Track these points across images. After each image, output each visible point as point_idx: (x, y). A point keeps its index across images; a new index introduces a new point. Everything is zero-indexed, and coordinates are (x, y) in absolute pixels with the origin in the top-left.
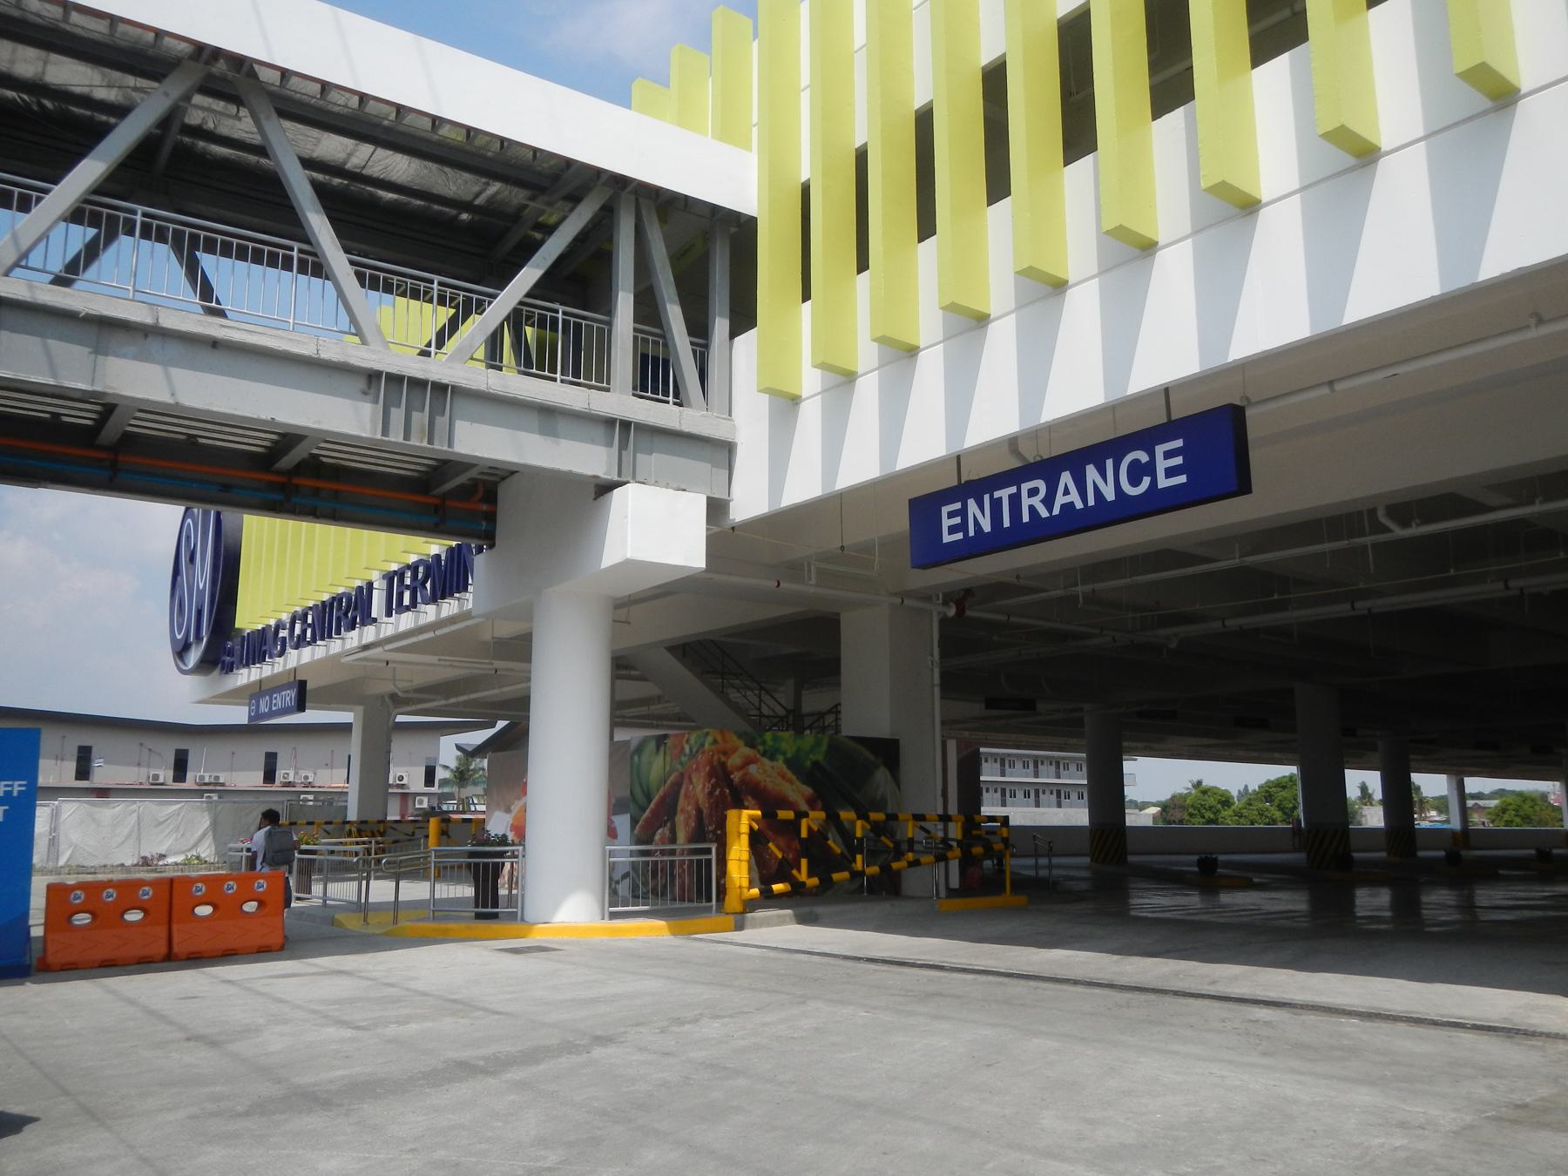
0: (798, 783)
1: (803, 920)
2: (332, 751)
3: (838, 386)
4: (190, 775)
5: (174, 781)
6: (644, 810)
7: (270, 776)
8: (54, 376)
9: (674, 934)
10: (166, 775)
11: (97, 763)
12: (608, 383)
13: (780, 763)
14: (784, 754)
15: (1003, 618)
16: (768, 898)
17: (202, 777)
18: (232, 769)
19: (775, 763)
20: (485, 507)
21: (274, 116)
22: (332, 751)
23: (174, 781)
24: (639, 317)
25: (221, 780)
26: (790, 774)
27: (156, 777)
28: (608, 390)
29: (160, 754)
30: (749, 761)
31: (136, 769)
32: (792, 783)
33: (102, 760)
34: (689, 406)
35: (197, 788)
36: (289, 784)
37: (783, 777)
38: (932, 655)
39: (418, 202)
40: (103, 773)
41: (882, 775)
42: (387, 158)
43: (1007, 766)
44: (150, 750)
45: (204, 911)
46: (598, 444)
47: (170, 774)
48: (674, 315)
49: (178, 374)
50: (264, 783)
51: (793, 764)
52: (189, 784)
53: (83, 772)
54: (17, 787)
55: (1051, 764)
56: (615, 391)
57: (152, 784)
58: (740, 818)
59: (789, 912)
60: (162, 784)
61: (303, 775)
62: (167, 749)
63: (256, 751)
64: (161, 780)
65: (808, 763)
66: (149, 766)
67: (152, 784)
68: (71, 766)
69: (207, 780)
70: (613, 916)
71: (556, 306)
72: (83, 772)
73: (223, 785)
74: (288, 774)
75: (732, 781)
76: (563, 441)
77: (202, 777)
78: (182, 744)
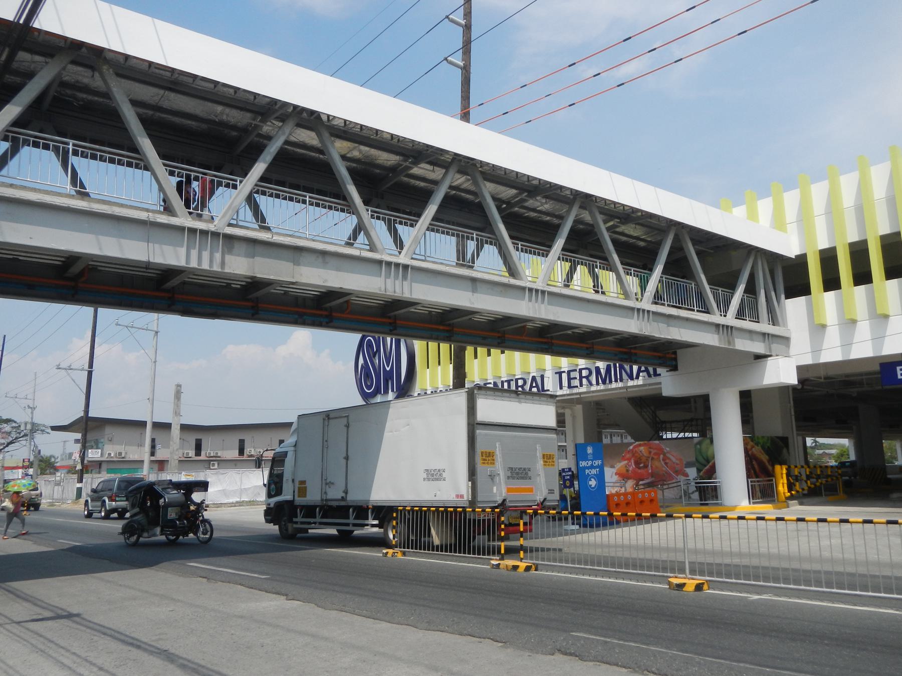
0: (764, 454)
1: (801, 504)
2: (271, 438)
3: (846, 323)
4: (203, 453)
5: (195, 456)
6: (705, 466)
7: (241, 452)
8: (671, 337)
9: (774, 509)
10: (192, 453)
11: (158, 447)
12: (758, 319)
13: (760, 448)
14: (760, 443)
15: (811, 388)
16: (792, 498)
17: (210, 453)
18: (223, 449)
19: (758, 448)
20: (673, 356)
21: (482, 179)
22: (271, 438)
23: (195, 456)
24: (746, 291)
25: (219, 455)
26: (762, 451)
27: (188, 454)
28: (759, 322)
29: (188, 442)
30: (753, 447)
32: (763, 454)
33: (160, 445)
34: (778, 325)
35: (207, 459)
36: (251, 456)
37: (761, 452)
38: (790, 403)
39: (536, 214)
41: (785, 451)
42: (507, 190)
43: (624, 438)
46: (761, 342)
47: (194, 452)
48: (773, 294)
49: (682, 330)
50: (239, 455)
51: (763, 447)
52: (203, 457)
55: (618, 436)
56: (763, 323)
57: (186, 458)
58: (782, 469)
59: (796, 501)
60: (190, 457)
61: (258, 451)
62: (233, 439)
64: (190, 456)
65: (766, 447)
67: (186, 458)
69: (212, 455)
70: (754, 503)
71: (631, 268)
73: (219, 457)
74: (251, 450)
75: (749, 454)
76: (755, 342)
78: (199, 436)
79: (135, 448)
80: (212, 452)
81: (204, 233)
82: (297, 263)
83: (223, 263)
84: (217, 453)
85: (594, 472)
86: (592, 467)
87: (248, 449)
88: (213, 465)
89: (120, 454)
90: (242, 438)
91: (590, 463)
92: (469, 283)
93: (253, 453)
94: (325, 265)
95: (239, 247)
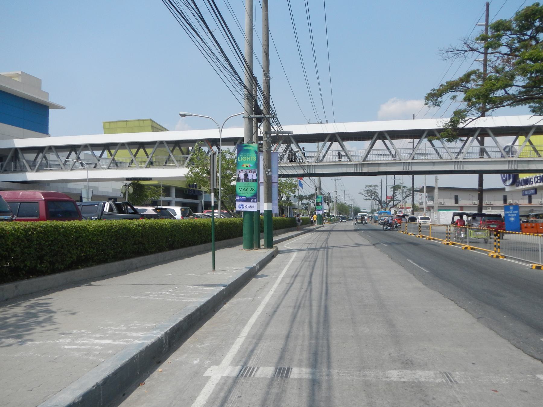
11: (459, 200)
17: (487, 203)
18: (494, 200)
25: (492, 203)
27: (475, 203)
31: (469, 201)
40: (461, 202)
44: (472, 196)
45: (541, 227)
53: (456, 201)
54: (517, 212)
63: (501, 195)
66: (472, 200)
68: (453, 201)
69: (488, 203)
72: (456, 201)
77: (487, 203)
79: (448, 200)
80: (488, 202)
81: (357, 164)
82: (379, 167)
83: (362, 170)
84: (491, 203)
85: (513, 215)
86: (512, 214)
87: (509, 201)
88: (489, 209)
89: (441, 203)
90: (505, 195)
91: (511, 212)
92: (432, 163)
93: (512, 203)
94: (387, 166)
95: (365, 166)
